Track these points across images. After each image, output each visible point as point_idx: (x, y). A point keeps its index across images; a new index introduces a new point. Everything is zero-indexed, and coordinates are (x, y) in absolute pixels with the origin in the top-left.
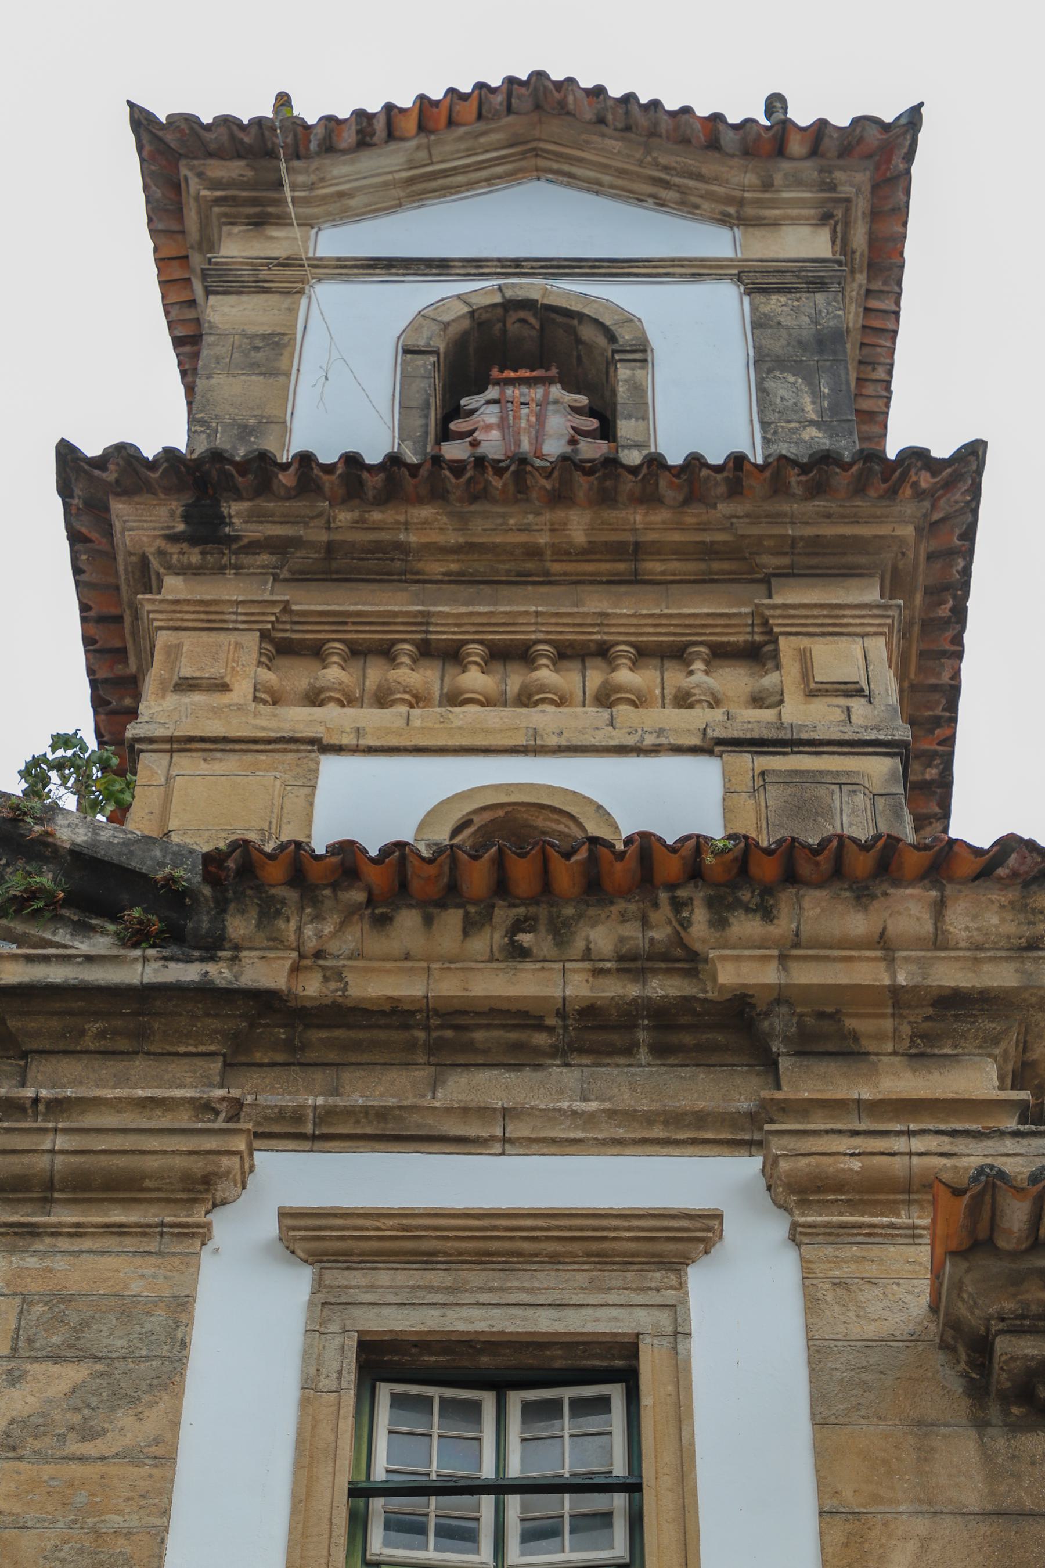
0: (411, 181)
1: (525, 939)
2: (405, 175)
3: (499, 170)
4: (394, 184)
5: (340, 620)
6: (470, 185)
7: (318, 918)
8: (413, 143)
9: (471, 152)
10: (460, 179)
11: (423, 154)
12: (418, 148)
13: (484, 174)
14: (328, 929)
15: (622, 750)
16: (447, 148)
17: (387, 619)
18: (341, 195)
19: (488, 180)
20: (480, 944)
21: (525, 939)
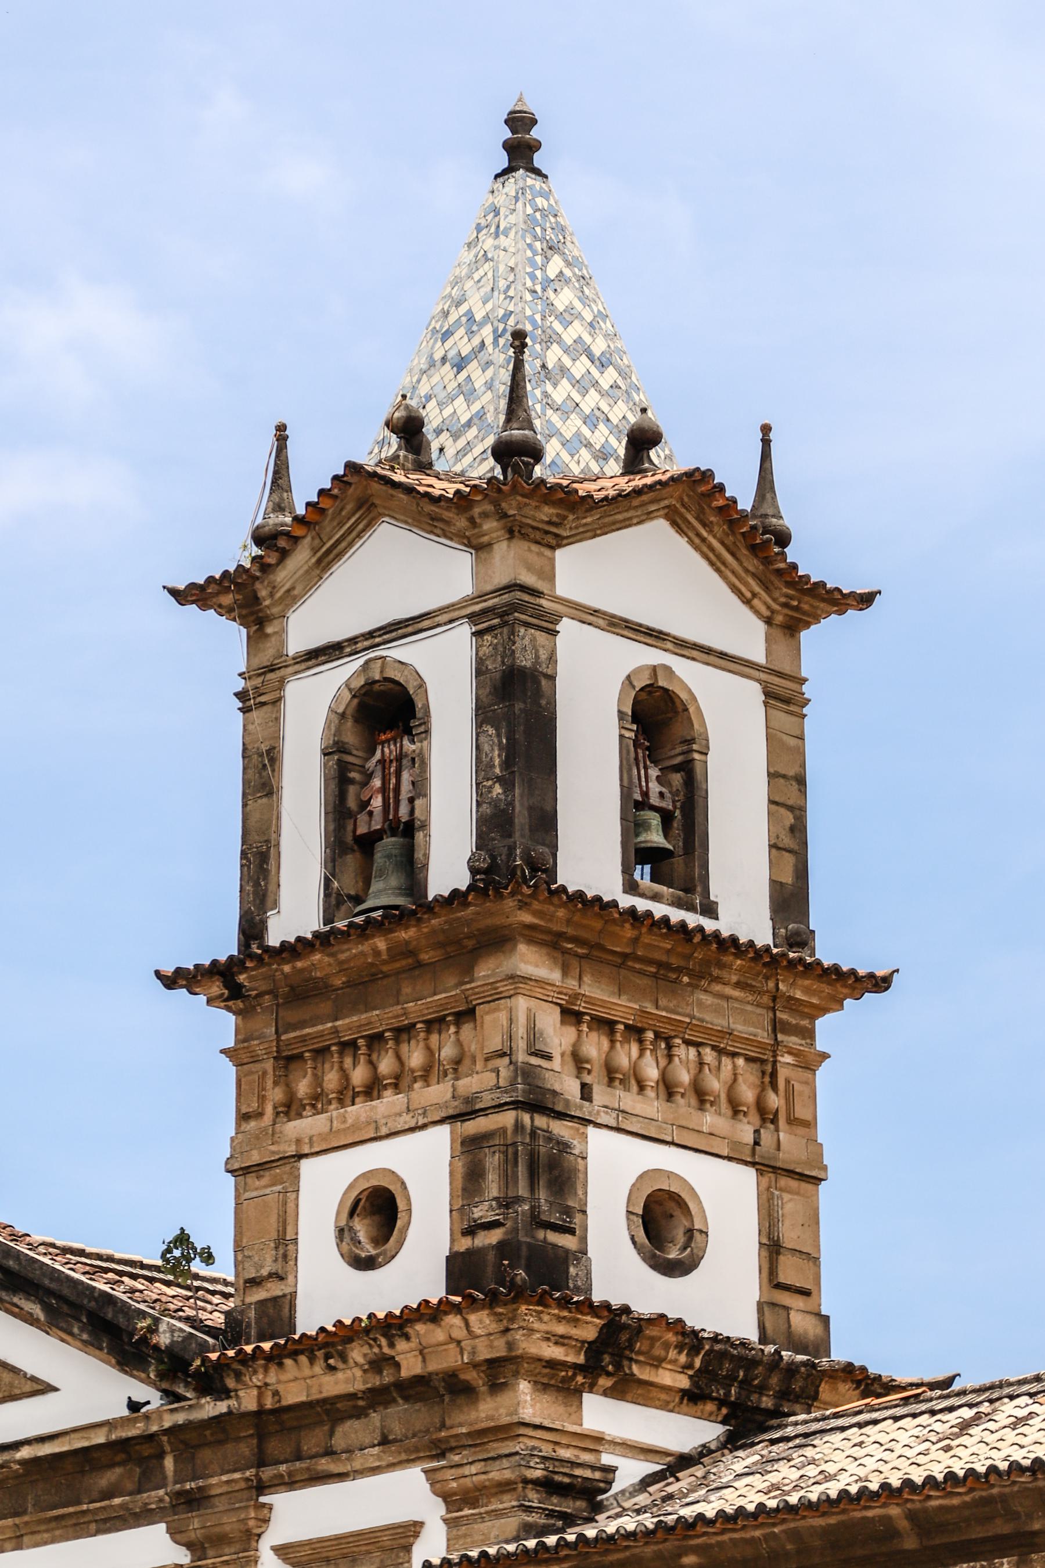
0: (319, 561)
1: (331, 1361)
2: (314, 560)
3: (361, 526)
4: (311, 569)
5: (303, 1039)
6: (351, 545)
7: (255, 1372)
8: (308, 539)
9: (341, 524)
10: (343, 545)
11: (317, 541)
12: (313, 538)
13: (354, 534)
14: (261, 1377)
15: (412, 1130)
16: (328, 529)
17: (320, 1035)
18: (288, 591)
19: (359, 536)
20: (318, 1369)
21: (331, 1361)
